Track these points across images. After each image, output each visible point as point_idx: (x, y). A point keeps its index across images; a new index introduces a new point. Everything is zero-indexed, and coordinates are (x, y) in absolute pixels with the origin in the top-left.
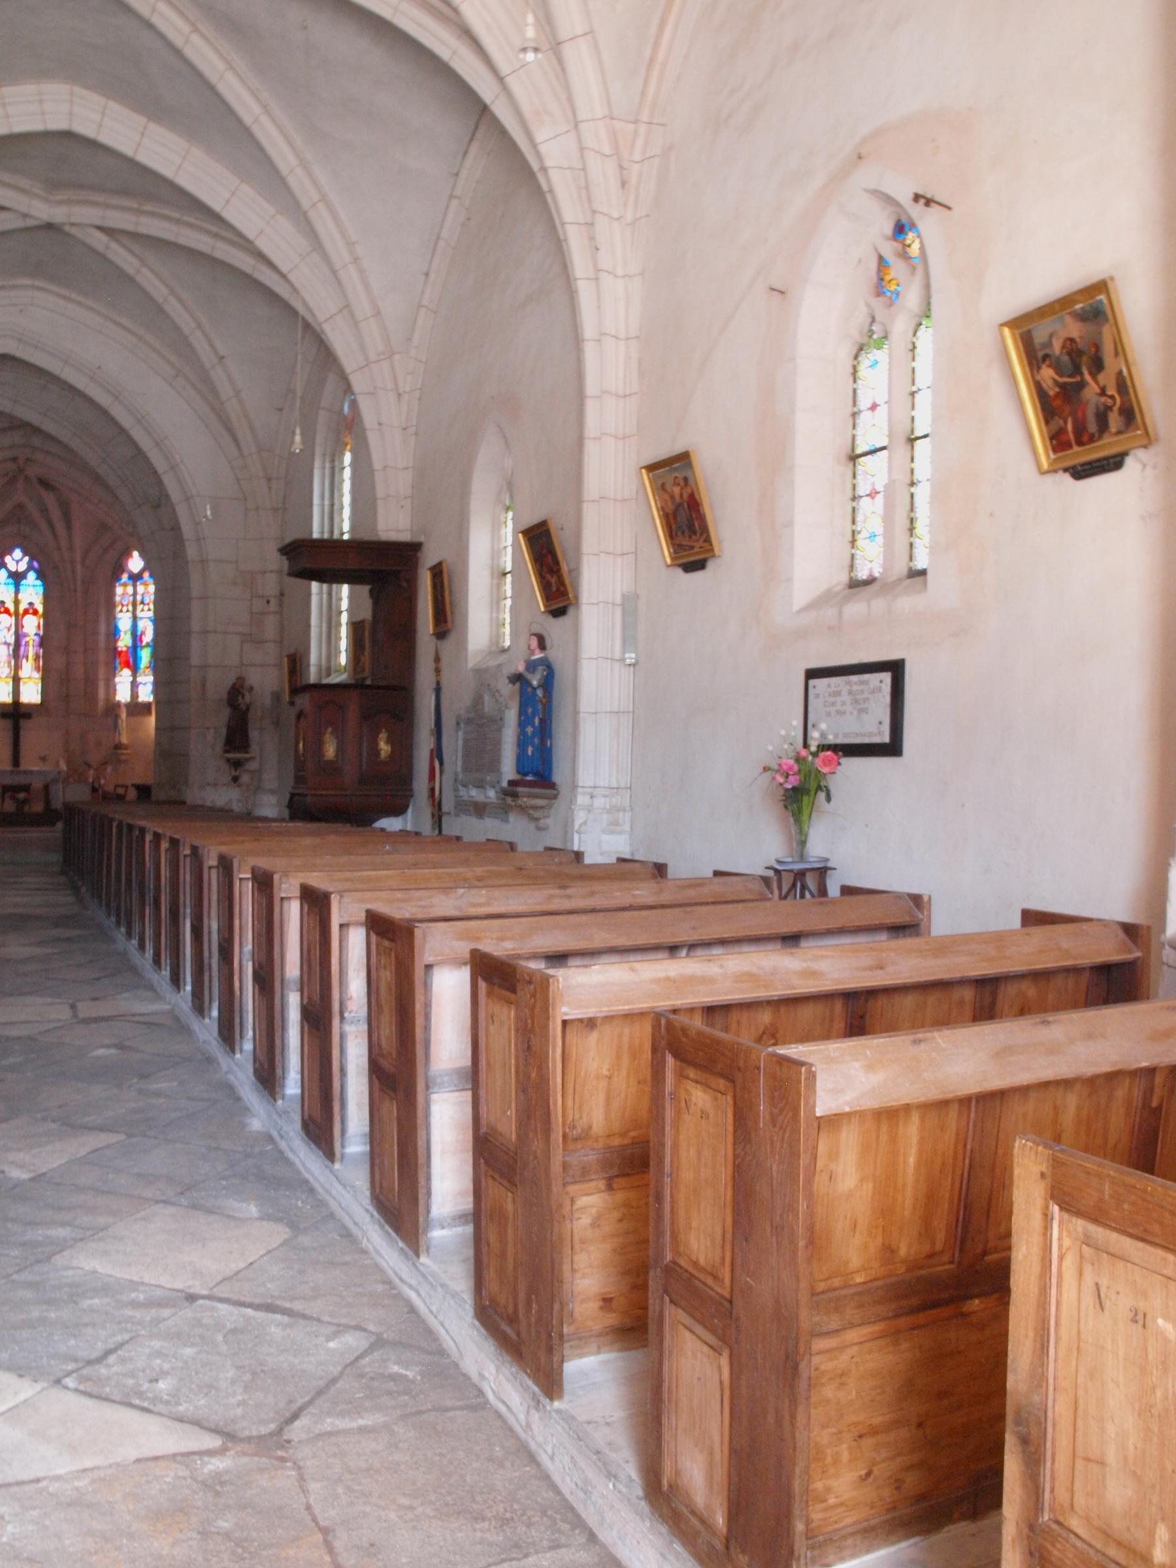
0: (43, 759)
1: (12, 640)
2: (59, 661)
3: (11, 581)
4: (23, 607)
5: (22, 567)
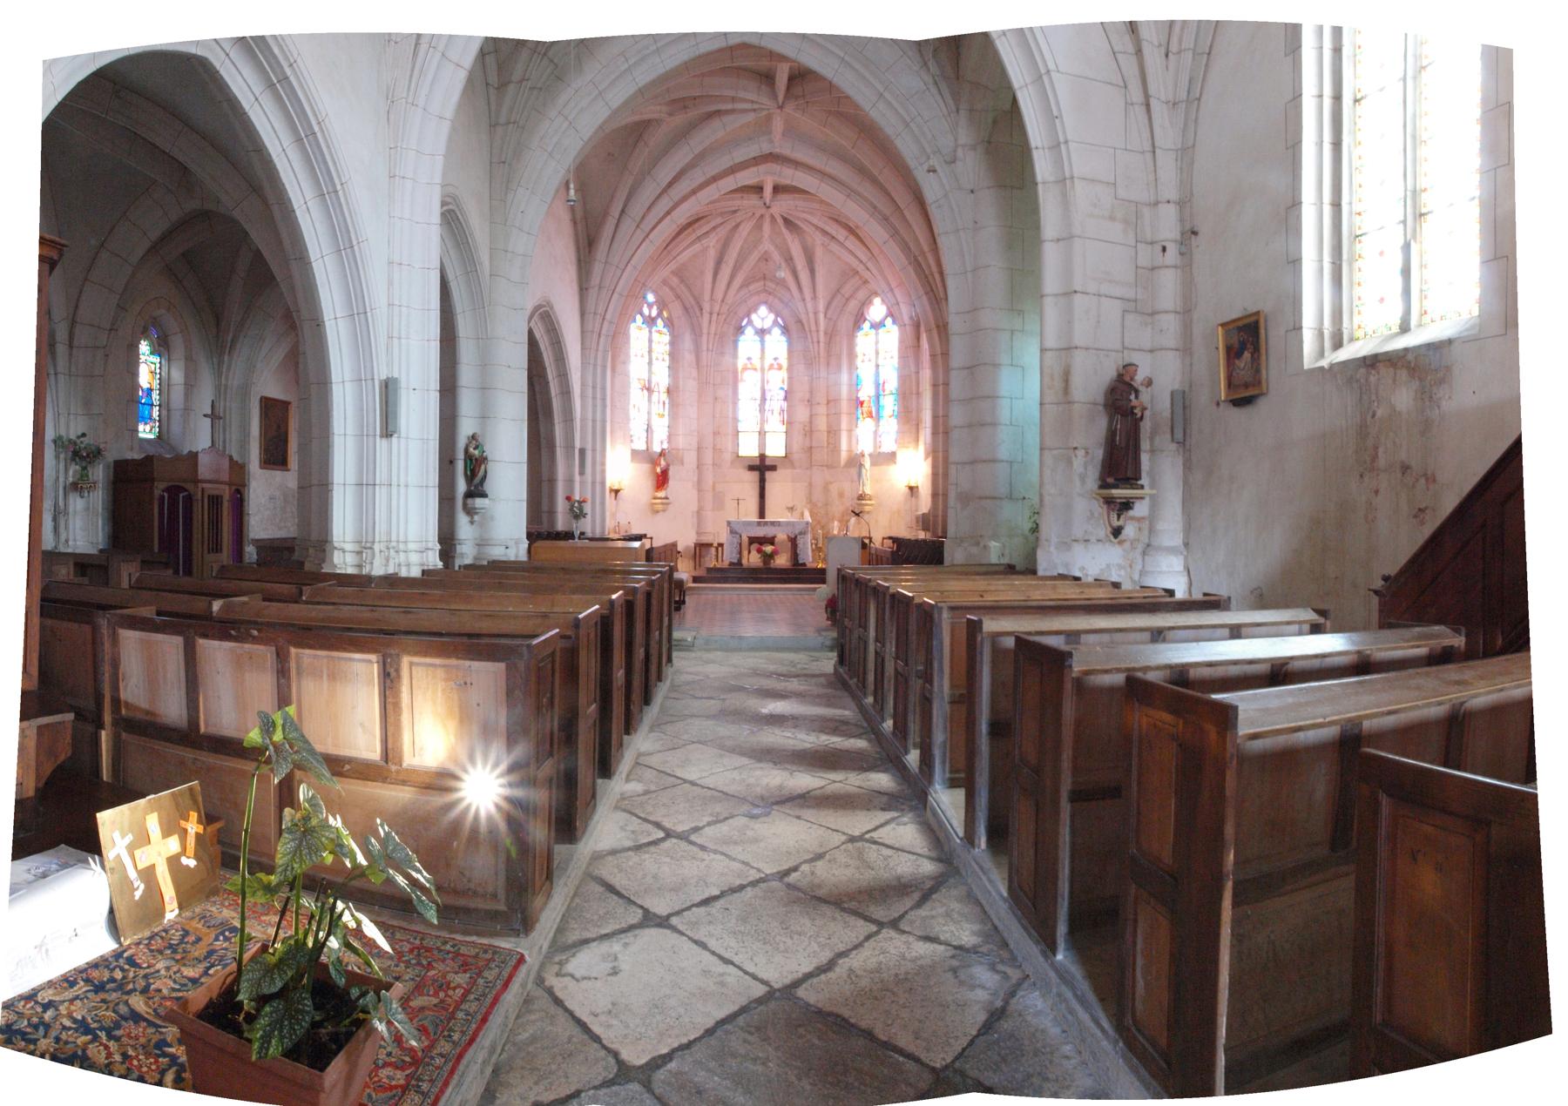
0: (791, 509)
1: (758, 396)
2: (802, 414)
4: (768, 361)
5: (768, 323)
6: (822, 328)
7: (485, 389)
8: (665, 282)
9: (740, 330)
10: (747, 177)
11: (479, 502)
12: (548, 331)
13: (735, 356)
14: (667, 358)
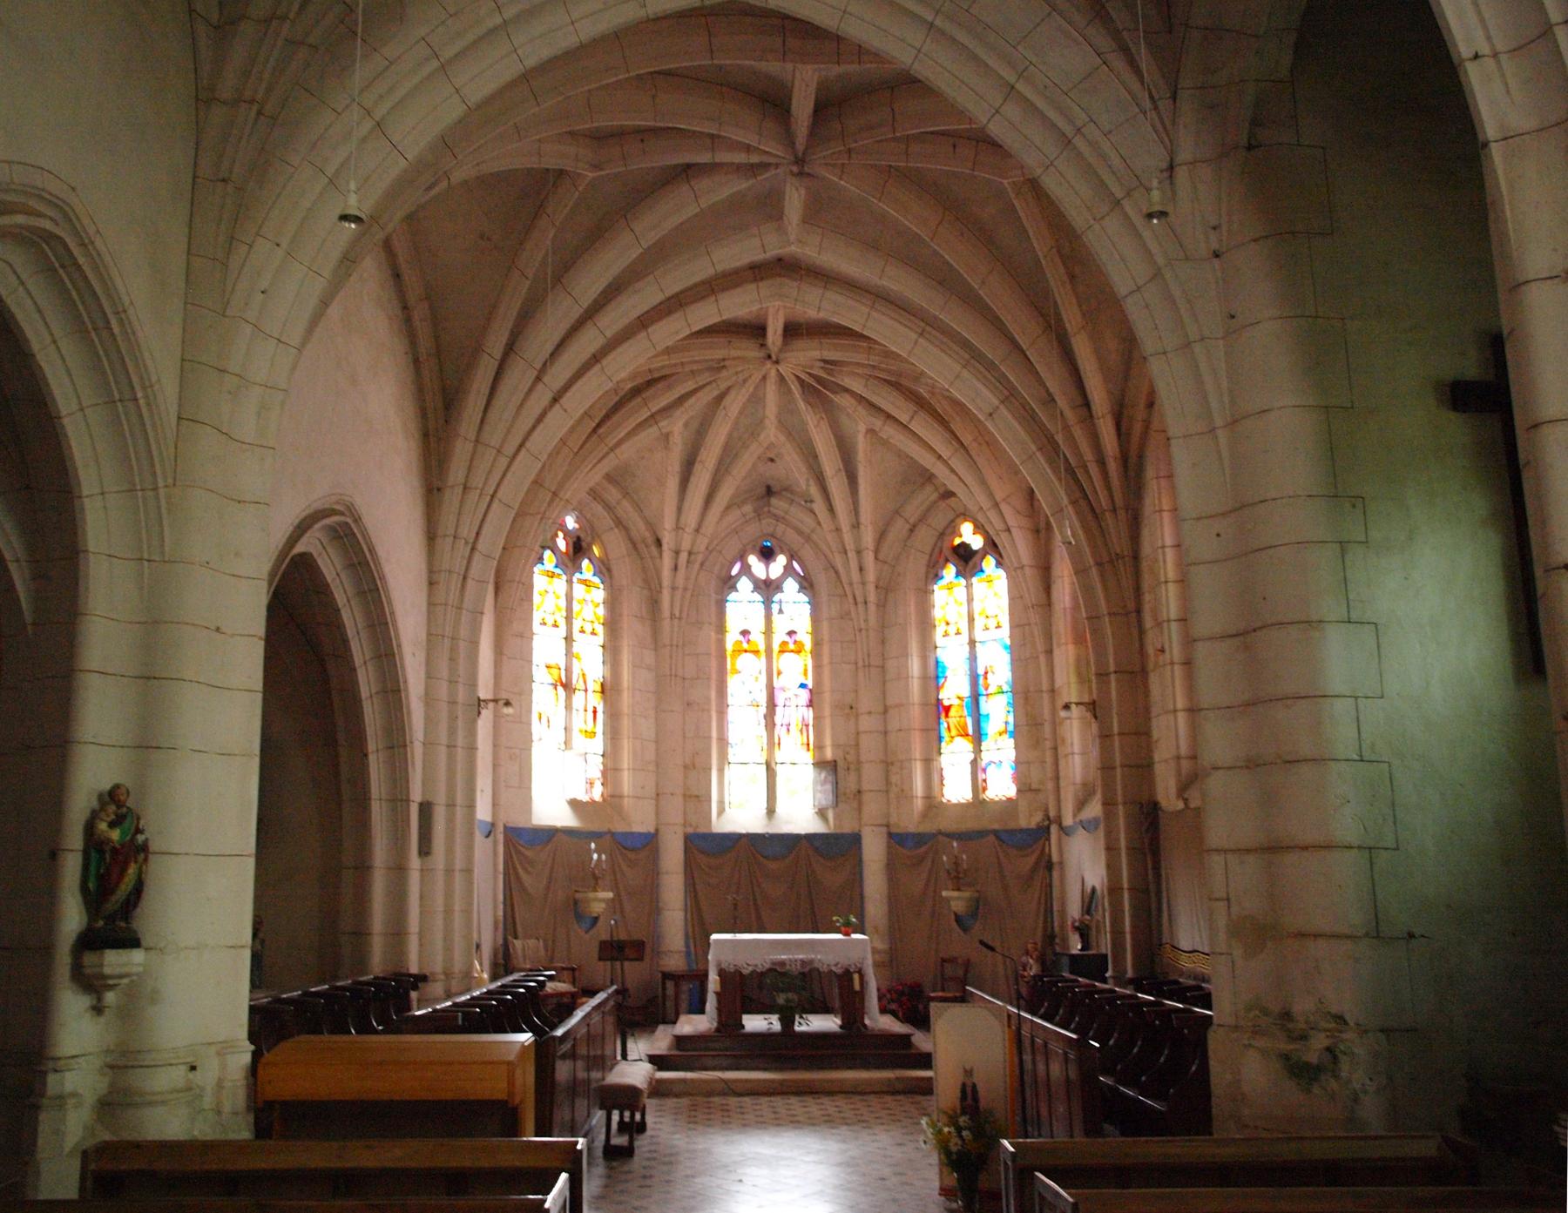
1: (762, 699)
3: (758, 597)
6: (871, 576)
7: (151, 680)
8: (594, 494)
9: (729, 584)
10: (738, 305)
11: (113, 960)
12: (351, 566)
13: (721, 629)
14: (600, 630)
